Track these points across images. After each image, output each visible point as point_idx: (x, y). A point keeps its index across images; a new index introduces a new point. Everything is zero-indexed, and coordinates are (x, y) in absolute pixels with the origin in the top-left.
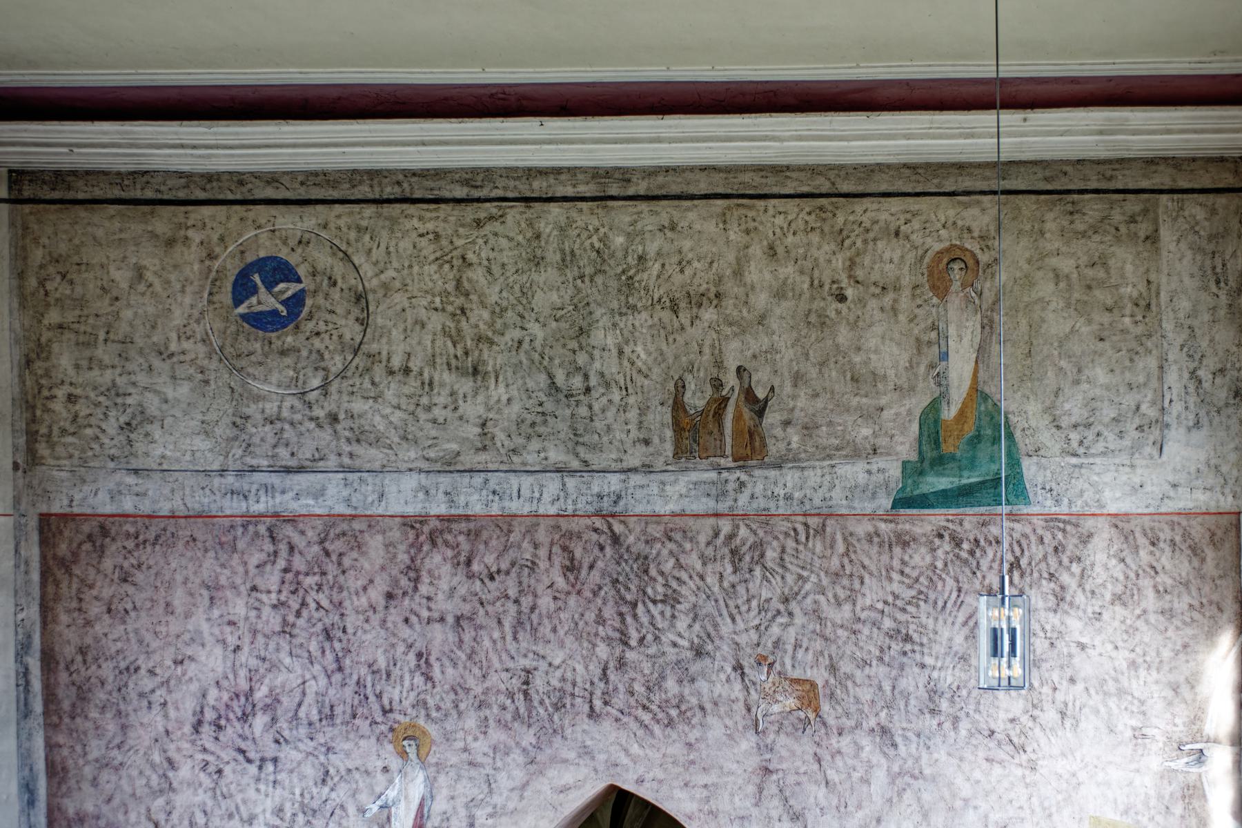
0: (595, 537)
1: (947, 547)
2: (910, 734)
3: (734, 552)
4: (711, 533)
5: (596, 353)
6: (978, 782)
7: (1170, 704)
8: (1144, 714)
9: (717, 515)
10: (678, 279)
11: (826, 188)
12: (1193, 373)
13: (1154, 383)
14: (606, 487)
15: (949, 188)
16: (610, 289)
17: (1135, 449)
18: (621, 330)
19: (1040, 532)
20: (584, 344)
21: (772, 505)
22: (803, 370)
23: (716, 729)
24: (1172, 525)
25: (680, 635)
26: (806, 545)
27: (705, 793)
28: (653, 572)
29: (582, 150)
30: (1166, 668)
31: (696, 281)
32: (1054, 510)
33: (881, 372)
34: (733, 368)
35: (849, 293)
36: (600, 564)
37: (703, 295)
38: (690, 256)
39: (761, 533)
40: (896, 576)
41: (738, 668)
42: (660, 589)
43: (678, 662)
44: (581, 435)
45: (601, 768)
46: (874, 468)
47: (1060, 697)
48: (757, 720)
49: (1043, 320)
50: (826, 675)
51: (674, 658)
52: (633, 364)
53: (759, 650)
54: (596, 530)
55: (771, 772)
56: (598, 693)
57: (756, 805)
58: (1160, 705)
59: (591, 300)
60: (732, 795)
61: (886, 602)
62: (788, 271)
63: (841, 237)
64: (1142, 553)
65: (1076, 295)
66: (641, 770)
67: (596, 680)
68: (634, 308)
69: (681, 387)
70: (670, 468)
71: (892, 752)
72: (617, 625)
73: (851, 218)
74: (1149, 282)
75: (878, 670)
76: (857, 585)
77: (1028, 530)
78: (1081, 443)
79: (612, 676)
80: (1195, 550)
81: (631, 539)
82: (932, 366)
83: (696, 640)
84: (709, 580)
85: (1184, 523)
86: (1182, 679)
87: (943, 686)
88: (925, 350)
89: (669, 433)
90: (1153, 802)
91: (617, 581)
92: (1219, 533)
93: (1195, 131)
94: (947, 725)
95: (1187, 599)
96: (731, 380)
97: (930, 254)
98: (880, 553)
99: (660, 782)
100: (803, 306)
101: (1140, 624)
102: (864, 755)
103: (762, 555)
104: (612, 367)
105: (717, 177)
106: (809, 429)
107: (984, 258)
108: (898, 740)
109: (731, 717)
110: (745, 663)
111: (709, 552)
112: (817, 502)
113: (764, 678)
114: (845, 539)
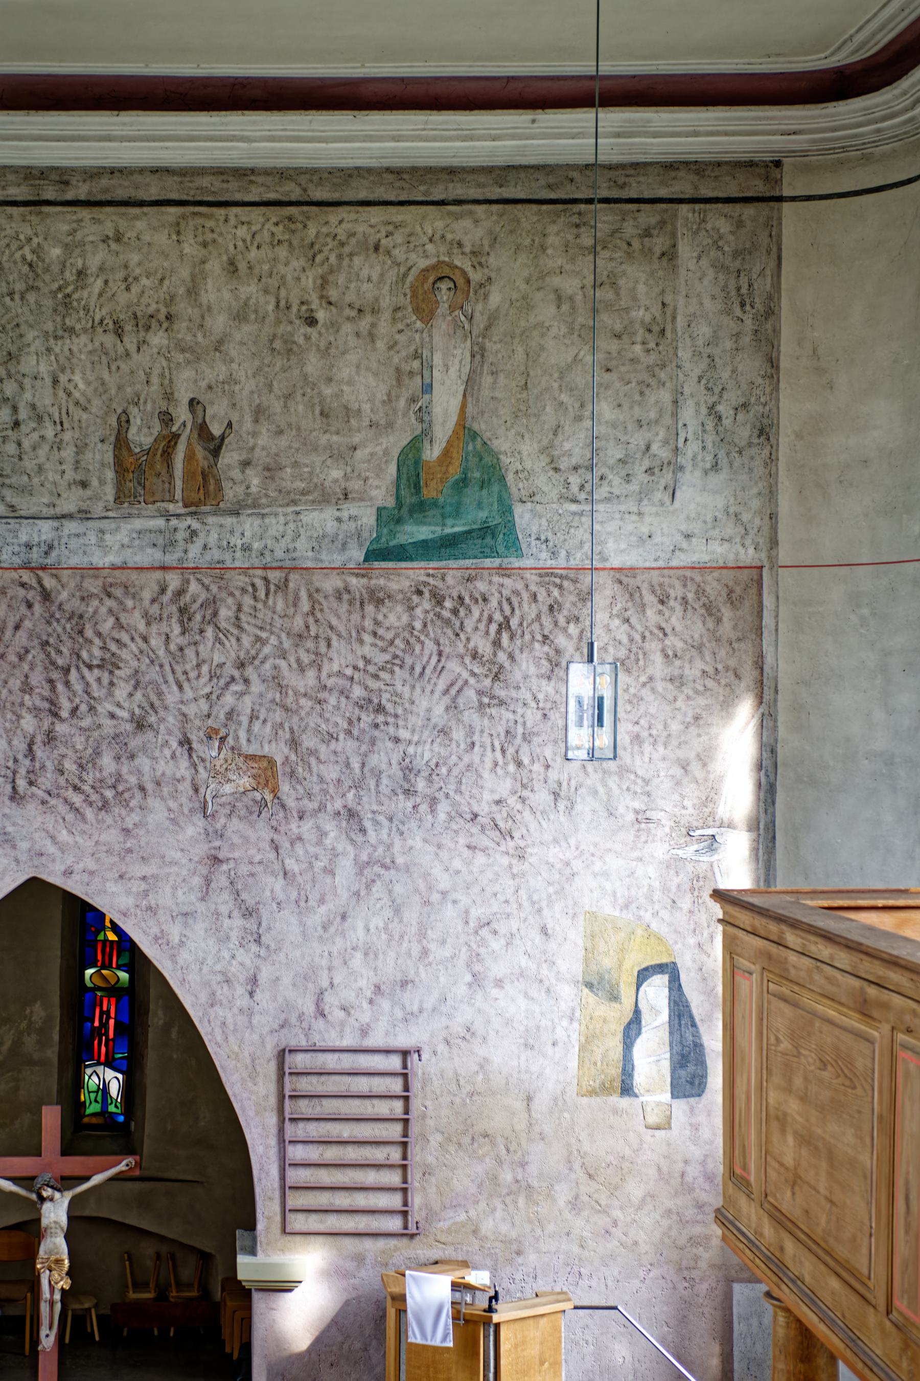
0: (22, 592)
1: (427, 605)
2: (381, 818)
3: (182, 611)
4: (156, 588)
5: (27, 382)
6: (458, 872)
7: (678, 783)
8: (649, 795)
9: (164, 568)
10: (123, 298)
11: (296, 194)
12: (712, 408)
13: (667, 420)
14: (35, 536)
15: (437, 195)
16: (44, 309)
17: (643, 494)
18: (56, 355)
19: (533, 588)
20: (13, 371)
21: (227, 557)
22: (265, 404)
23: (158, 813)
24: (684, 582)
25: (119, 705)
26: (265, 603)
27: (143, 886)
28: (89, 633)
29: (17, 148)
30: (674, 742)
31: (144, 300)
32: (549, 563)
33: (356, 406)
34: (185, 401)
35: (321, 315)
36: (27, 624)
37: (152, 316)
38: (138, 271)
39: (214, 589)
40: (367, 638)
41: (185, 742)
42: (97, 652)
43: (116, 736)
44: (7, 476)
45: (23, 857)
46: (345, 515)
47: (553, 775)
48: (205, 802)
49: (542, 348)
50: (286, 750)
51: (111, 731)
52: (69, 395)
53: (210, 722)
54: (23, 585)
55: (220, 861)
56: (23, 771)
57: (203, 899)
58: (667, 784)
59: (21, 320)
60: (174, 888)
61: (355, 668)
62: (250, 289)
63: (312, 252)
64: (649, 612)
65: (580, 320)
66: (70, 860)
67: (20, 757)
68: (71, 331)
69: (124, 422)
70: (110, 514)
71: (359, 838)
72: (46, 693)
73: (324, 230)
74: (664, 304)
75: (347, 745)
76: (323, 649)
77: (520, 586)
78: (582, 488)
79: (39, 752)
80: (710, 610)
81: (64, 595)
82: (413, 400)
83: (137, 711)
84: (153, 642)
85: (698, 579)
86: (692, 755)
87: (419, 763)
88: (406, 380)
89: (110, 475)
90: (657, 895)
91: (47, 643)
92: (738, 590)
93: (726, 134)
94: (424, 808)
95: (699, 665)
96: (182, 414)
97: (414, 272)
98: (350, 612)
99: (92, 873)
100: (268, 330)
101: (645, 693)
102: (328, 842)
103: (215, 614)
104: (45, 399)
105: (171, 181)
106: (271, 471)
107: (476, 277)
108: (368, 824)
109: (175, 798)
110: (193, 737)
111: (155, 610)
112: (279, 554)
113: (214, 754)
114: (310, 596)
